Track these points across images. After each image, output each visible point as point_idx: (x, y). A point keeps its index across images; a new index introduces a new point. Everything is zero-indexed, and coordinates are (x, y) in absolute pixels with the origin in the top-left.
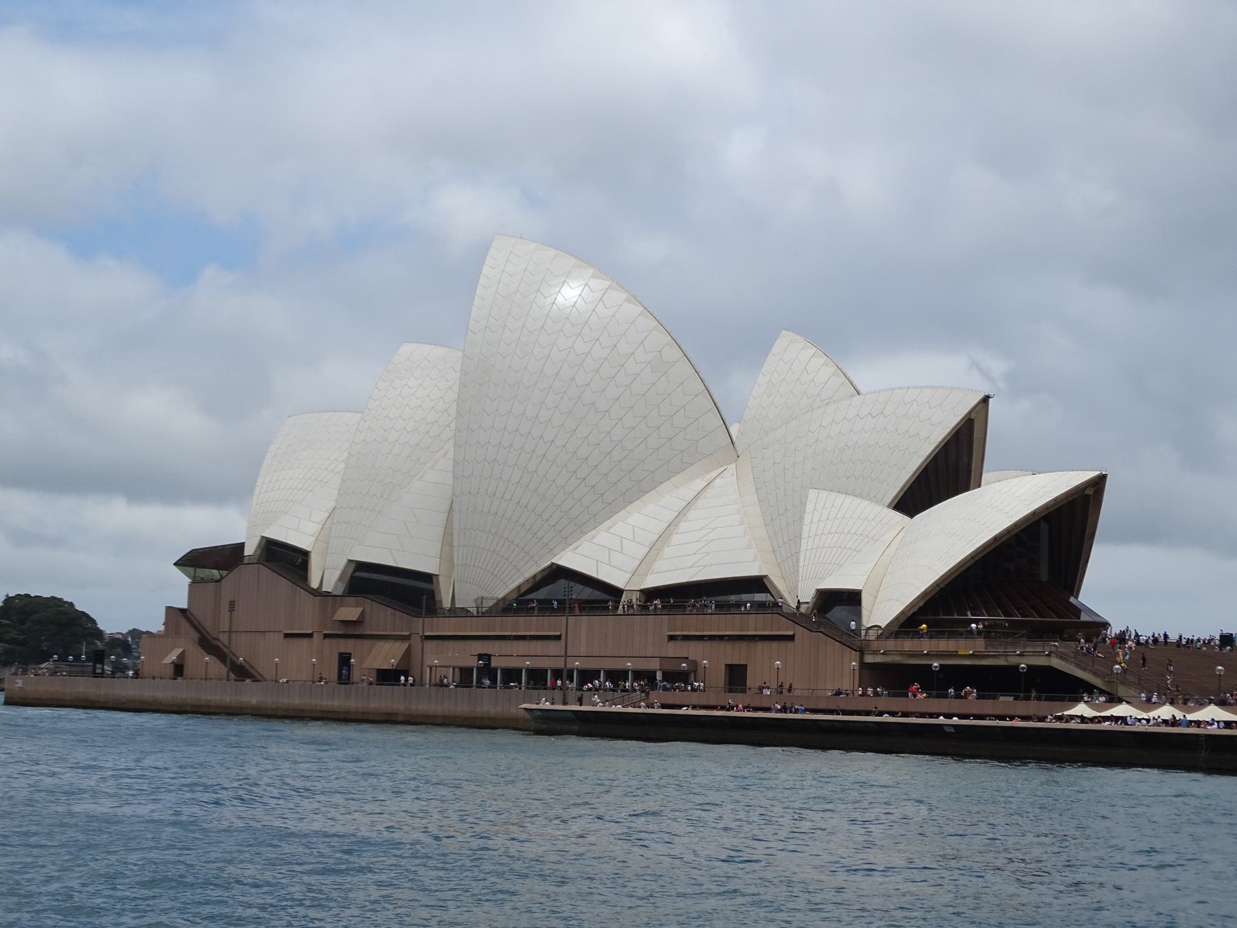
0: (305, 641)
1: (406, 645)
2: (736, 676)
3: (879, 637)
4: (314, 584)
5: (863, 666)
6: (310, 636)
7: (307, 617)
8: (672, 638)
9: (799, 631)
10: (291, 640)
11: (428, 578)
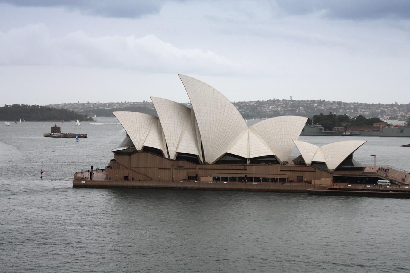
0: (170, 170)
1: (195, 170)
4: (167, 157)
5: (333, 176)
6: (170, 169)
7: (168, 165)
8: (280, 171)
10: (161, 170)
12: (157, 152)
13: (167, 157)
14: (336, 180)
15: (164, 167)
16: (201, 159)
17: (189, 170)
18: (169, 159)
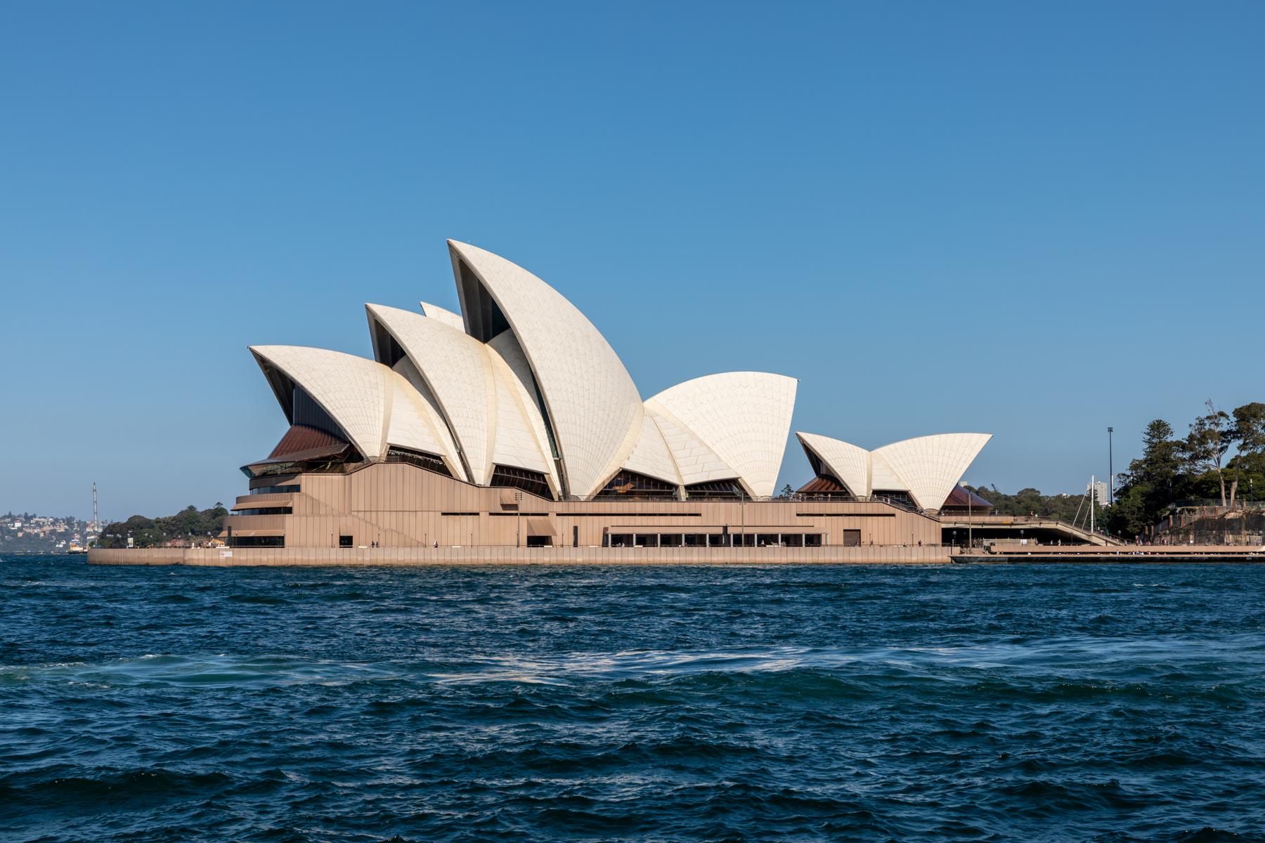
2: (853, 537)
3: (939, 514)
7: (471, 500)
9: (897, 512)
11: (540, 475)
12: (432, 463)
13: (465, 479)
14: (949, 537)
16: (556, 486)
18: (471, 480)
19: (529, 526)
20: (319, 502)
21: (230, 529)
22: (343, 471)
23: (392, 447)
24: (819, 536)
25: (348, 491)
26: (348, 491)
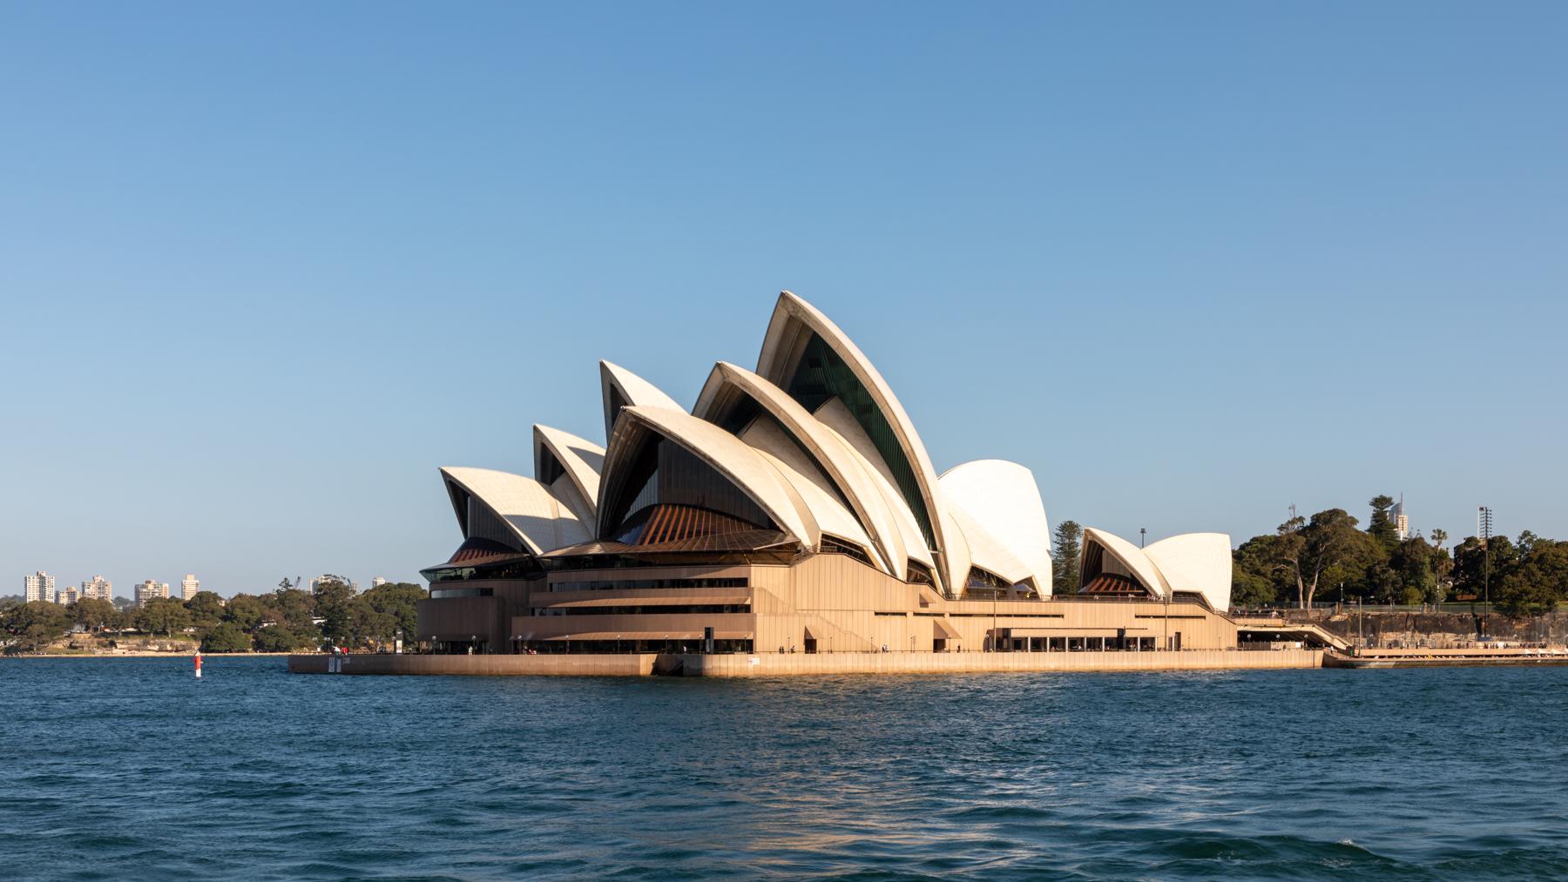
15: (888, 610)
17: (938, 619)
18: (894, 574)
19: (937, 627)
20: (777, 599)
21: (708, 632)
22: (788, 563)
23: (824, 536)
24: (1153, 639)
25: (792, 583)
26: (792, 583)
